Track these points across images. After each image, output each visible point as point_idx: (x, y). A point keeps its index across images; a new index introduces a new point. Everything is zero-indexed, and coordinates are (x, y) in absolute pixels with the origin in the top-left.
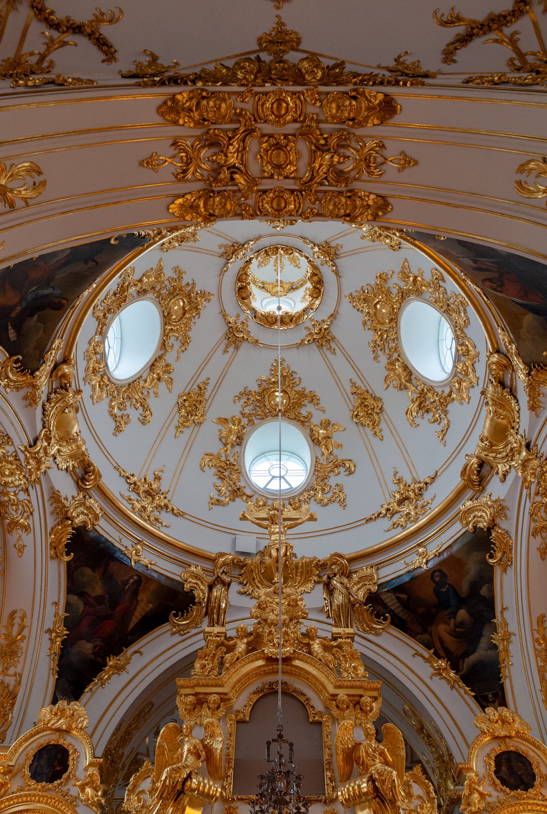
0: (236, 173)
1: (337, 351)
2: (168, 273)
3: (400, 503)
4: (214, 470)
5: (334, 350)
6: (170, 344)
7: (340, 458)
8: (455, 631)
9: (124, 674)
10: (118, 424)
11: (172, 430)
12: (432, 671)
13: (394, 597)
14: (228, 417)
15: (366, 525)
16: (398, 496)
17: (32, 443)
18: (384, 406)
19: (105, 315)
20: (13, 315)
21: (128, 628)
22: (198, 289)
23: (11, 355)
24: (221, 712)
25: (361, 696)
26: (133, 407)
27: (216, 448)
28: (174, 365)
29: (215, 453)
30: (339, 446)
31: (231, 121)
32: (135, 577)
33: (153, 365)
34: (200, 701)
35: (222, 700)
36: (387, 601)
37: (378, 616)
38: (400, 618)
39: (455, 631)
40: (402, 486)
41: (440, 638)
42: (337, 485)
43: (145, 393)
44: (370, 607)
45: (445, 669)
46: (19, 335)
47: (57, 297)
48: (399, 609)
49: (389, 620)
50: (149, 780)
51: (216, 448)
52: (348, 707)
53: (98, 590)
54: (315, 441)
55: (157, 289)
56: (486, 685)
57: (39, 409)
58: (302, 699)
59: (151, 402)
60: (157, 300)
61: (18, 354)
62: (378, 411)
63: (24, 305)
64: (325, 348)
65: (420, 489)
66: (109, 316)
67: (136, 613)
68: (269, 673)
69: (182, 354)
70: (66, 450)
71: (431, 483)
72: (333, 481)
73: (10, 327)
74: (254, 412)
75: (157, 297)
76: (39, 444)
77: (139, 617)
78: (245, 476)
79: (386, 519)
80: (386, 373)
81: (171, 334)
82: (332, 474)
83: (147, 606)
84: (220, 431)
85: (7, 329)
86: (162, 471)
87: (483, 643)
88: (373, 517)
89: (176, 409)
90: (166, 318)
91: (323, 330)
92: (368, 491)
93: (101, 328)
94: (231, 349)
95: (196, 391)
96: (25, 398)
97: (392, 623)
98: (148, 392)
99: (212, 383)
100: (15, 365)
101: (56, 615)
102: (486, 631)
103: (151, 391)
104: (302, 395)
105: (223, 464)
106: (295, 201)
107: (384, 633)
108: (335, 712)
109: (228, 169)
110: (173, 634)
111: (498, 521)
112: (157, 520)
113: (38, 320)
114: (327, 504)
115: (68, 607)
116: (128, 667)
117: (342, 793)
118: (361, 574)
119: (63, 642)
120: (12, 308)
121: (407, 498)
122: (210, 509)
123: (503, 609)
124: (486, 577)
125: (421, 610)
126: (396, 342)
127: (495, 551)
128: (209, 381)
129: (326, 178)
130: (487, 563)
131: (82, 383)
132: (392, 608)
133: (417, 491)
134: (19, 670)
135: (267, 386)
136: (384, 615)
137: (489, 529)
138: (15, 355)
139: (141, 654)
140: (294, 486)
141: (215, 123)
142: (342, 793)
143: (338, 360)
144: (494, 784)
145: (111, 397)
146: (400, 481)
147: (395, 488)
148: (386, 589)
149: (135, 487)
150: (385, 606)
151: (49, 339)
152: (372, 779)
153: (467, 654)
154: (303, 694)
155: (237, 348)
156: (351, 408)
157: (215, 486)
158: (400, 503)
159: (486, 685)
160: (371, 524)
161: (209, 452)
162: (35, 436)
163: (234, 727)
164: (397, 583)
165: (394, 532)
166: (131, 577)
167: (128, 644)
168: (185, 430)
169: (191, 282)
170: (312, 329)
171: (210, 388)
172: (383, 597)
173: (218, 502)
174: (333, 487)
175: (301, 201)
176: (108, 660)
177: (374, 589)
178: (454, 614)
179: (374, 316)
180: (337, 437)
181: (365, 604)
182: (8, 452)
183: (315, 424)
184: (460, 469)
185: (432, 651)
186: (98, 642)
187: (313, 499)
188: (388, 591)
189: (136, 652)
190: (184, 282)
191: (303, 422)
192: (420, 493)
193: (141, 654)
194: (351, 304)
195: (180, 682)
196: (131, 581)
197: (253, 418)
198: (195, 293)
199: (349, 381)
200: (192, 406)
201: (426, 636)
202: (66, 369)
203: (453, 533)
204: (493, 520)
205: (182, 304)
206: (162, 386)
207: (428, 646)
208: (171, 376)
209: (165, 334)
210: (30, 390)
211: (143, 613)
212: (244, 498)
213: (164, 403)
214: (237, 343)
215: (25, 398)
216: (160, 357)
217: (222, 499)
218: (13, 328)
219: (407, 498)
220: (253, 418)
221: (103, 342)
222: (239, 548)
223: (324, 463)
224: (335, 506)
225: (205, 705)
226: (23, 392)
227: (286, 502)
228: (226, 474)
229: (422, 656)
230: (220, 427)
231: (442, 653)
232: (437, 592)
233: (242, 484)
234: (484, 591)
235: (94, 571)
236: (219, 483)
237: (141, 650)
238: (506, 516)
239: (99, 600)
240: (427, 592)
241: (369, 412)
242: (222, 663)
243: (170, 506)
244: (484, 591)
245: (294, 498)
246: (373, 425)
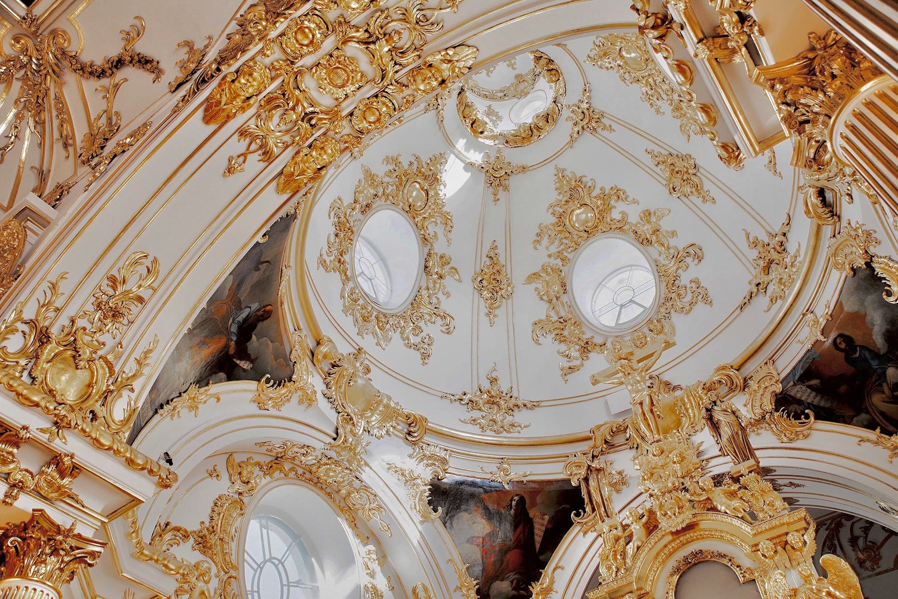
0: (311, 119)
1: (614, 126)
2: (380, 170)
3: (767, 269)
4: (551, 337)
5: (610, 126)
6: (432, 234)
7: (680, 248)
8: (894, 397)
10: (423, 351)
11: (484, 320)
12: (889, 453)
13: (804, 388)
14: (537, 269)
15: (743, 314)
16: (762, 263)
17: (335, 436)
18: (697, 162)
19: (339, 261)
20: (232, 351)
21: (535, 549)
22: (425, 159)
23: (259, 381)
25: (787, 534)
26: (429, 324)
27: (541, 311)
28: (448, 252)
29: (544, 317)
30: (674, 234)
31: (273, 79)
32: (516, 498)
33: (426, 267)
36: (798, 395)
37: (797, 417)
38: (823, 408)
39: (894, 397)
40: (761, 250)
41: (883, 414)
43: (434, 301)
44: (783, 411)
46: (252, 361)
47: (258, 310)
48: (818, 398)
51: (541, 311)
52: (776, 552)
54: (645, 242)
55: (380, 194)
57: (323, 403)
58: (725, 561)
59: (446, 305)
60: (388, 202)
61: (264, 375)
62: (694, 171)
63: (234, 338)
64: (599, 130)
66: (346, 257)
67: (536, 531)
68: (679, 547)
69: (450, 235)
70: (374, 418)
72: (685, 279)
73: (238, 362)
74: (562, 247)
75: (387, 199)
76: (341, 431)
77: (542, 534)
78: (586, 323)
79: (761, 296)
80: (678, 122)
81: (426, 224)
82: (680, 271)
83: (543, 519)
84: (536, 289)
85: (237, 365)
88: (746, 300)
89: (477, 295)
90: (410, 210)
91: (585, 111)
92: (726, 272)
93: (346, 275)
94: (501, 194)
95: (488, 263)
96: (301, 402)
97: (816, 418)
98: (438, 299)
99: (501, 244)
100: (268, 385)
103: (440, 295)
104: (604, 196)
105: (558, 325)
106: (384, 103)
109: (303, 120)
110: (585, 533)
111: (872, 250)
113: (258, 339)
118: (757, 378)
120: (227, 347)
121: (771, 262)
125: (843, 389)
126: (667, 82)
127: (890, 286)
128: (496, 244)
129: (396, 64)
130: (888, 305)
131: (358, 339)
132: (809, 401)
133: (778, 248)
135: (561, 210)
136: (803, 413)
137: (868, 264)
138: (262, 377)
139: (562, 568)
141: (260, 93)
143: (620, 136)
145: (399, 329)
146: (755, 244)
147: (753, 254)
148: (792, 383)
150: (800, 402)
151: (282, 344)
155: (506, 189)
156: (664, 182)
160: (747, 310)
161: (533, 320)
162: (333, 429)
164: (800, 372)
165: (776, 307)
166: (511, 500)
167: (543, 565)
168: (497, 312)
169: (413, 159)
170: (574, 117)
171: (501, 251)
172: (792, 394)
174: (689, 286)
175: (391, 98)
176: (531, 589)
177: (778, 388)
179: (625, 67)
180: (665, 225)
182: (317, 456)
183: (634, 222)
185: (878, 430)
186: (512, 576)
187: (672, 311)
188: (795, 385)
190: (405, 165)
191: (620, 228)
193: (562, 568)
194: (596, 67)
196: (514, 503)
197: (565, 254)
198: (425, 166)
199: (646, 154)
200: (493, 283)
201: (864, 416)
202: (324, 349)
204: (866, 252)
205: (418, 186)
206: (448, 281)
207: (871, 426)
208: (452, 264)
209: (419, 227)
210: (300, 393)
211: (544, 529)
212: (597, 348)
213: (460, 299)
214: (503, 182)
215: (301, 402)
216: (429, 255)
218: (241, 359)
219: (771, 262)
220: (565, 254)
221: (357, 285)
222: (614, 411)
223: (666, 262)
224: (700, 307)
226: (295, 398)
227: (646, 330)
228: (566, 333)
229: (868, 441)
230: (534, 285)
231: (891, 428)
233: (587, 336)
236: (563, 347)
237: (560, 564)
238: (878, 242)
240: (839, 365)
241: (685, 178)
243: (520, 404)
245: (650, 321)
246: (697, 190)
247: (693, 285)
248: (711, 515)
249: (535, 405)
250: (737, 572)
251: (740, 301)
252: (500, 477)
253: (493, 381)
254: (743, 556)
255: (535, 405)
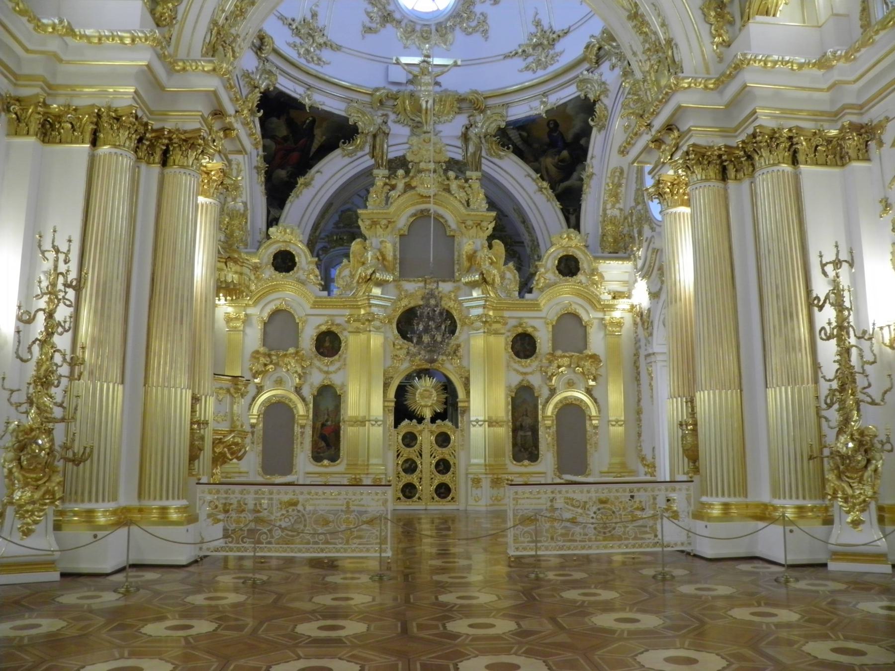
9: (310, 188)
24: (389, 229)
34: (374, 223)
35: (389, 222)
37: (503, 146)
42: (482, 14)
45: (545, 188)
49: (511, 149)
50: (348, 270)
53: (283, 131)
56: (570, 203)
65: (554, 40)
71: (563, 36)
86: (317, 6)
87: (575, 175)
101: (258, 155)
102: (579, 168)
107: (506, 158)
108: (464, 230)
111: (602, 97)
112: (319, 59)
114: (470, 34)
115: (265, 148)
116: (313, 183)
117: (465, 280)
119: (266, 173)
121: (541, 44)
122: (363, 37)
123: (592, 157)
124: (586, 132)
134: (244, 200)
136: (508, 145)
137: (595, 101)
140: (441, 8)
142: (465, 280)
144: (554, 273)
146: (538, 24)
147: (533, 29)
149: (297, 32)
150: (510, 139)
152: (482, 274)
153: (562, 181)
154: (442, 217)
157: (368, 13)
158: (535, 47)
159: (570, 203)
163: (398, 240)
173: (369, 30)
177: (503, 125)
178: (559, 152)
181: (495, 136)
184: (585, 45)
186: (289, 168)
187: (458, 28)
189: (318, 172)
192: (552, 43)
195: (359, 211)
201: (536, 164)
203: (568, 93)
207: (537, 171)
217: (374, 25)
224: (477, 36)
225: (378, 226)
227: (433, 28)
231: (545, 177)
232: (550, 134)
233: (391, 8)
234: (582, 142)
235: (279, 118)
236: (370, 8)
238: (607, 96)
239: (285, 139)
240: (542, 134)
242: (388, 198)
244: (582, 142)
247: (482, 18)
248: (447, 195)
249: (337, 48)
250: (448, 229)
251: (506, 51)
252: (307, 102)
253: (314, 15)
254: (452, 222)
255: (337, 48)
